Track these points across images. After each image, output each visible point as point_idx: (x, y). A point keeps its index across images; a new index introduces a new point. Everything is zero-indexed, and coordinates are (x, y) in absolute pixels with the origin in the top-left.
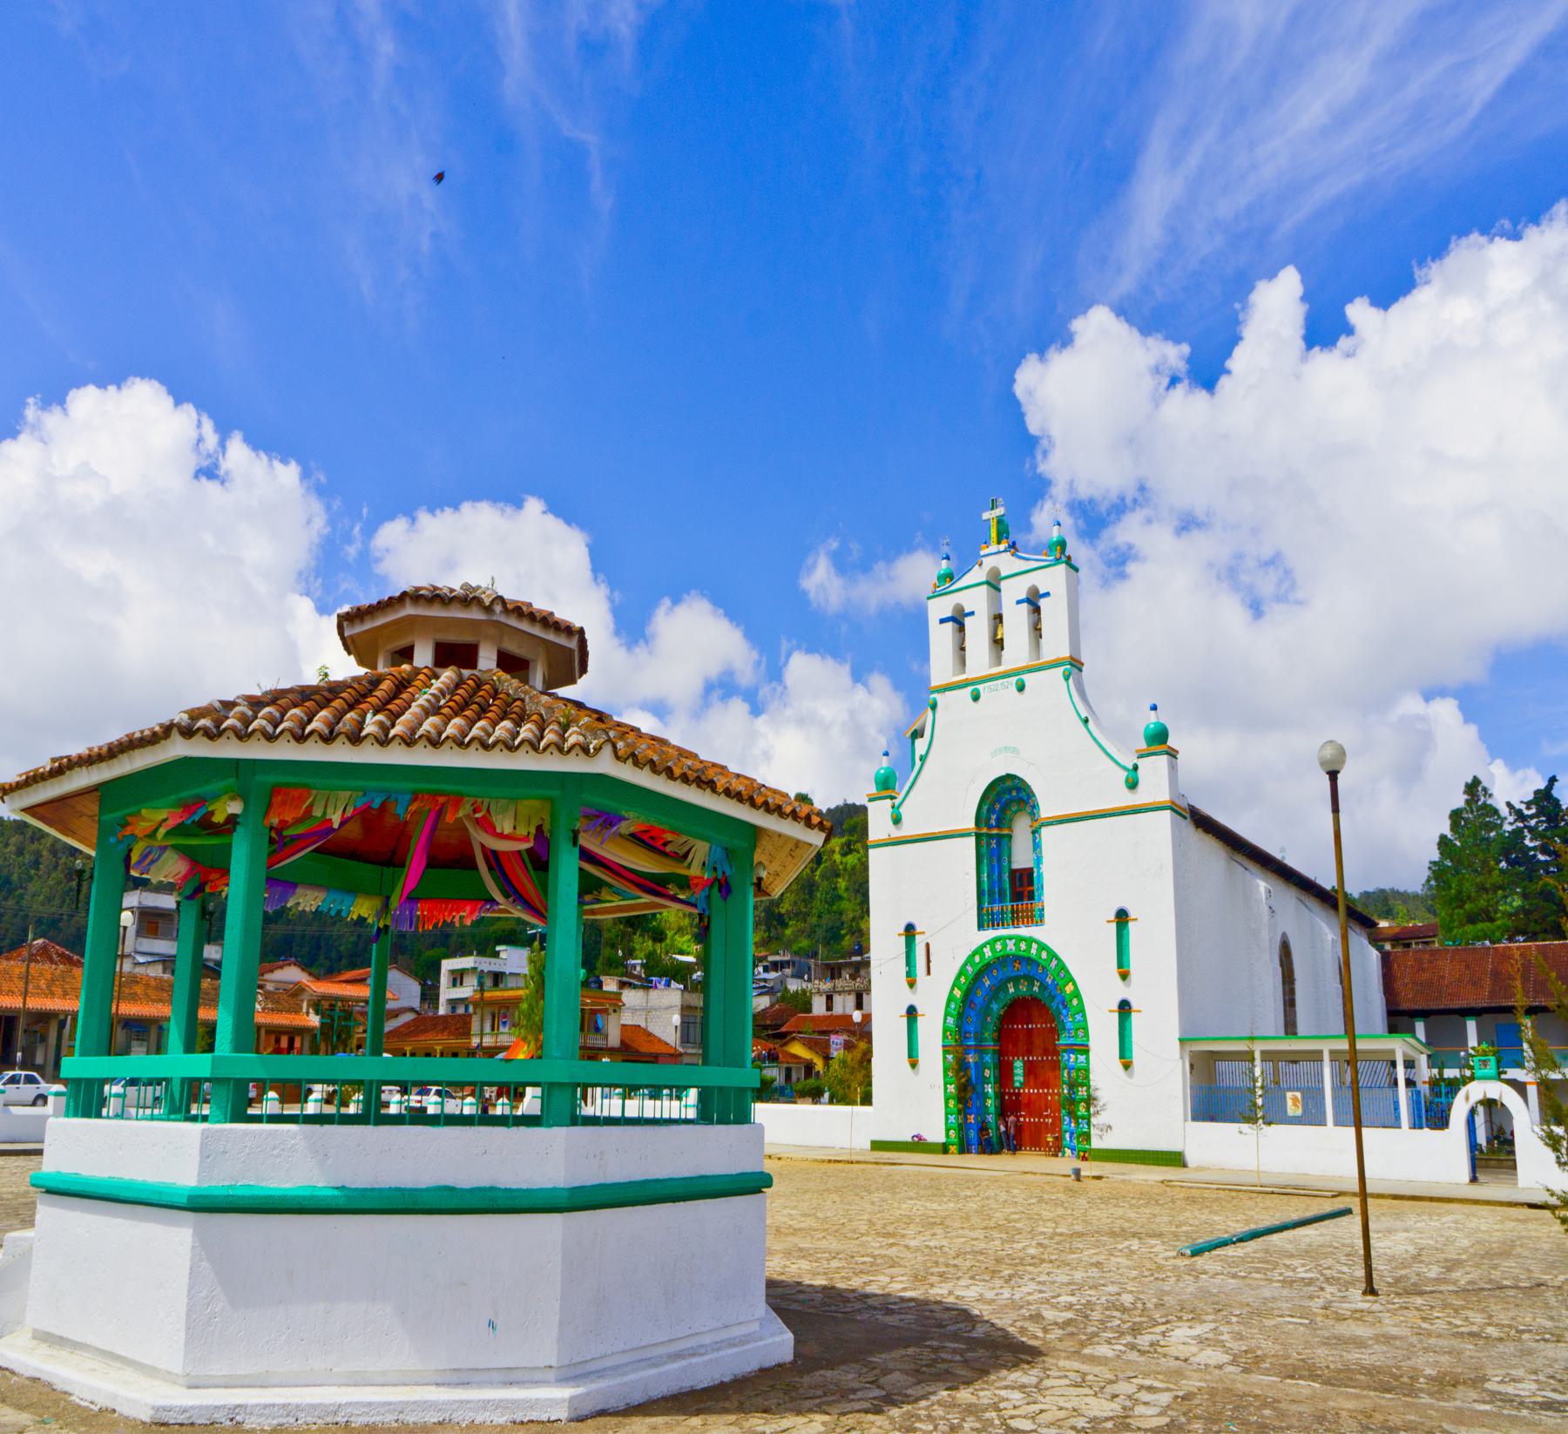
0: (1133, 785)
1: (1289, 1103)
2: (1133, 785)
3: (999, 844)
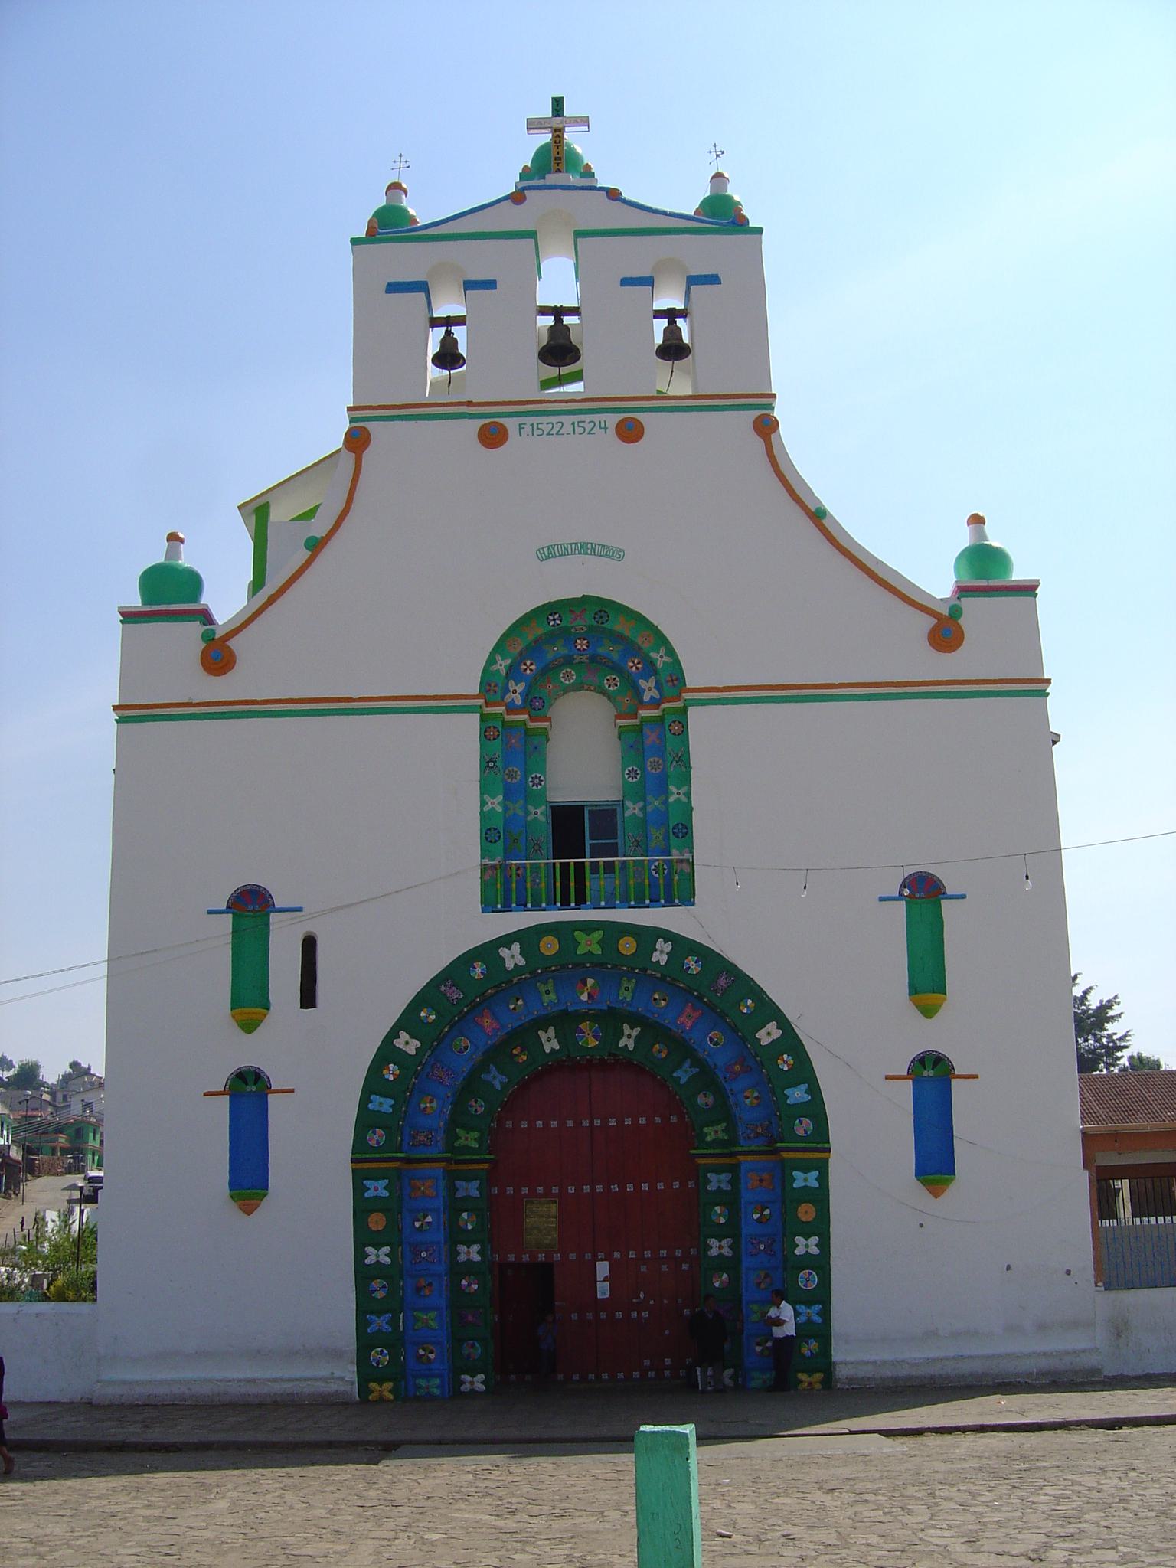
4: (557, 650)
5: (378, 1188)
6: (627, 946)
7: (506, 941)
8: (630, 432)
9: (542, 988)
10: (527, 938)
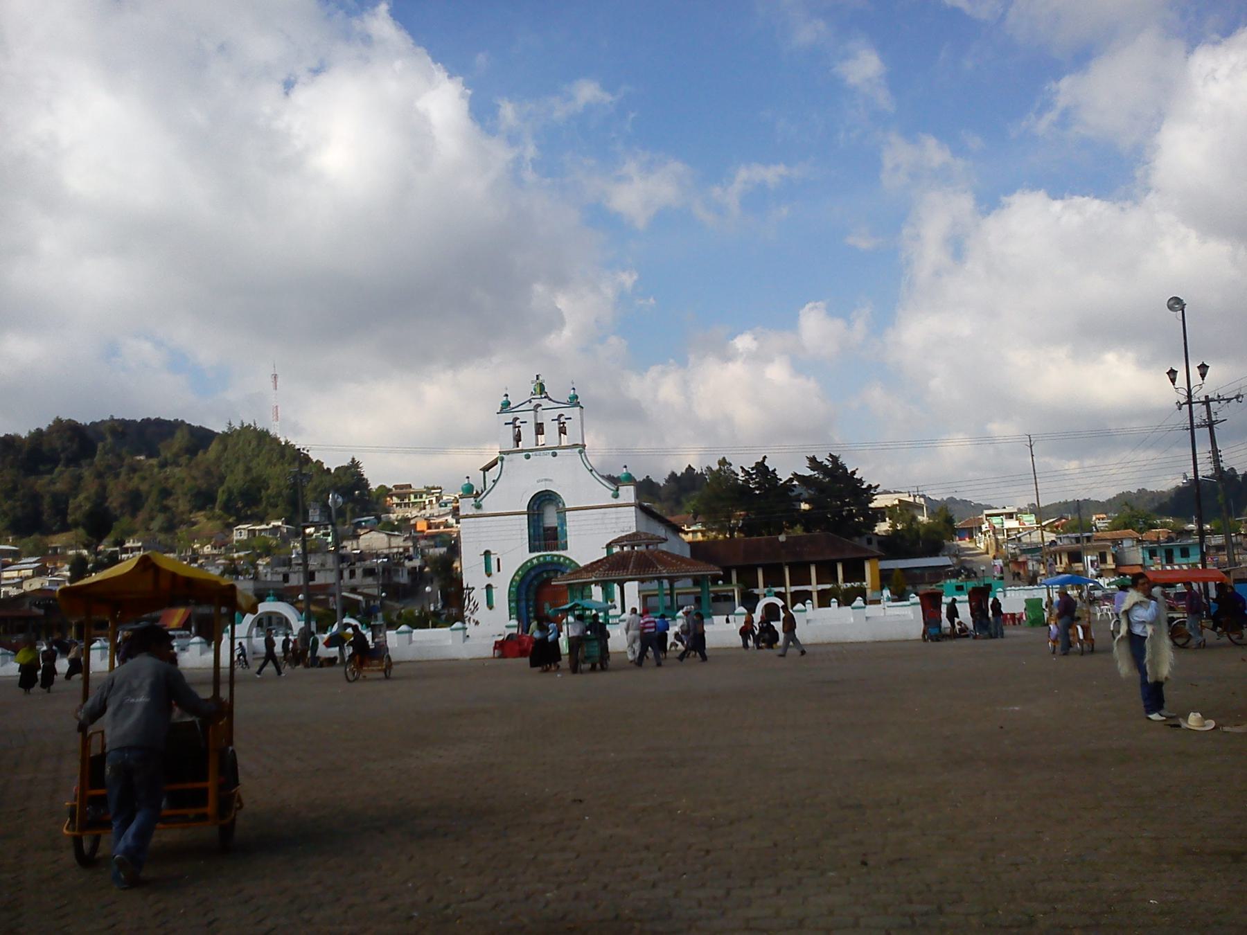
0: (616, 496)
2: (616, 496)
3: (538, 516)
5: (513, 604)
6: (555, 558)
7: (534, 558)
8: (555, 455)
10: (538, 558)
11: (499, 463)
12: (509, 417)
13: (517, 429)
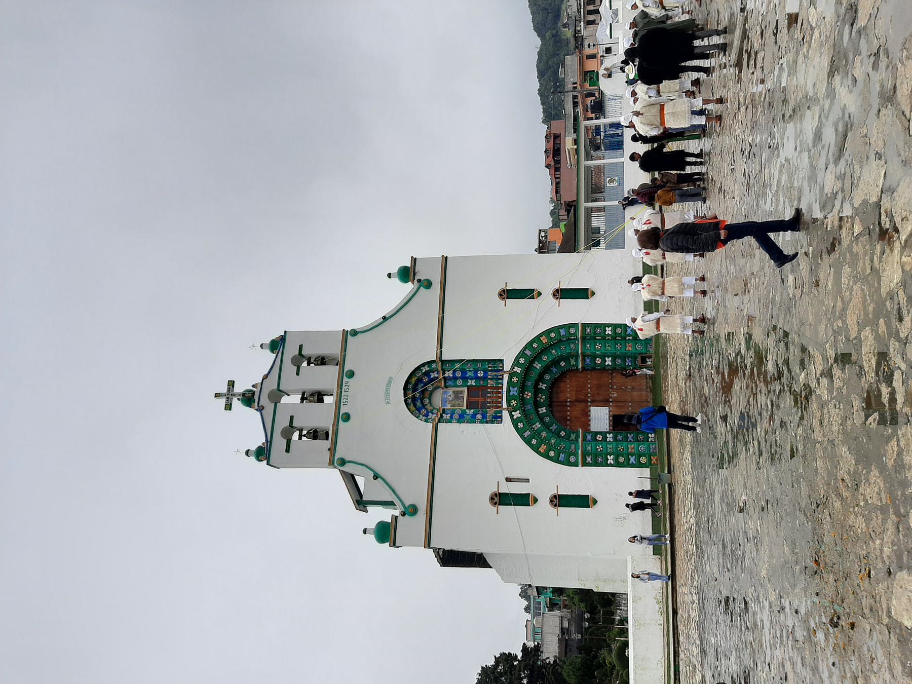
0: (428, 284)
1: (612, 185)
2: (428, 284)
4: (418, 404)
7: (512, 416)
8: (351, 374)
9: (535, 365)
11: (348, 468)
12: (279, 443)
13: (304, 439)
